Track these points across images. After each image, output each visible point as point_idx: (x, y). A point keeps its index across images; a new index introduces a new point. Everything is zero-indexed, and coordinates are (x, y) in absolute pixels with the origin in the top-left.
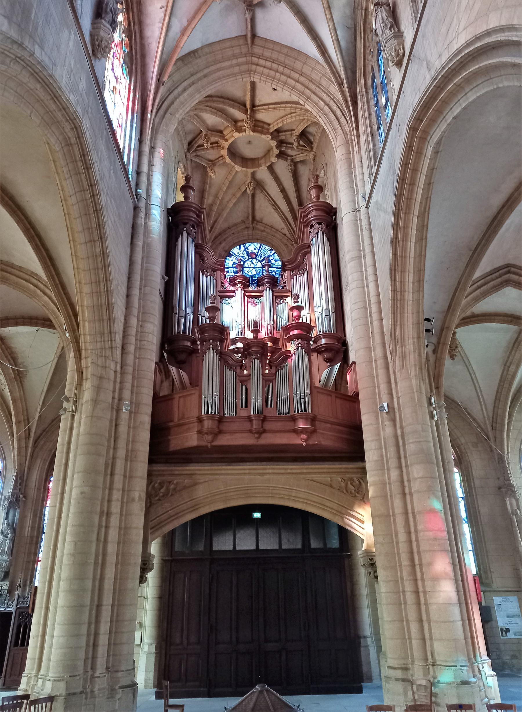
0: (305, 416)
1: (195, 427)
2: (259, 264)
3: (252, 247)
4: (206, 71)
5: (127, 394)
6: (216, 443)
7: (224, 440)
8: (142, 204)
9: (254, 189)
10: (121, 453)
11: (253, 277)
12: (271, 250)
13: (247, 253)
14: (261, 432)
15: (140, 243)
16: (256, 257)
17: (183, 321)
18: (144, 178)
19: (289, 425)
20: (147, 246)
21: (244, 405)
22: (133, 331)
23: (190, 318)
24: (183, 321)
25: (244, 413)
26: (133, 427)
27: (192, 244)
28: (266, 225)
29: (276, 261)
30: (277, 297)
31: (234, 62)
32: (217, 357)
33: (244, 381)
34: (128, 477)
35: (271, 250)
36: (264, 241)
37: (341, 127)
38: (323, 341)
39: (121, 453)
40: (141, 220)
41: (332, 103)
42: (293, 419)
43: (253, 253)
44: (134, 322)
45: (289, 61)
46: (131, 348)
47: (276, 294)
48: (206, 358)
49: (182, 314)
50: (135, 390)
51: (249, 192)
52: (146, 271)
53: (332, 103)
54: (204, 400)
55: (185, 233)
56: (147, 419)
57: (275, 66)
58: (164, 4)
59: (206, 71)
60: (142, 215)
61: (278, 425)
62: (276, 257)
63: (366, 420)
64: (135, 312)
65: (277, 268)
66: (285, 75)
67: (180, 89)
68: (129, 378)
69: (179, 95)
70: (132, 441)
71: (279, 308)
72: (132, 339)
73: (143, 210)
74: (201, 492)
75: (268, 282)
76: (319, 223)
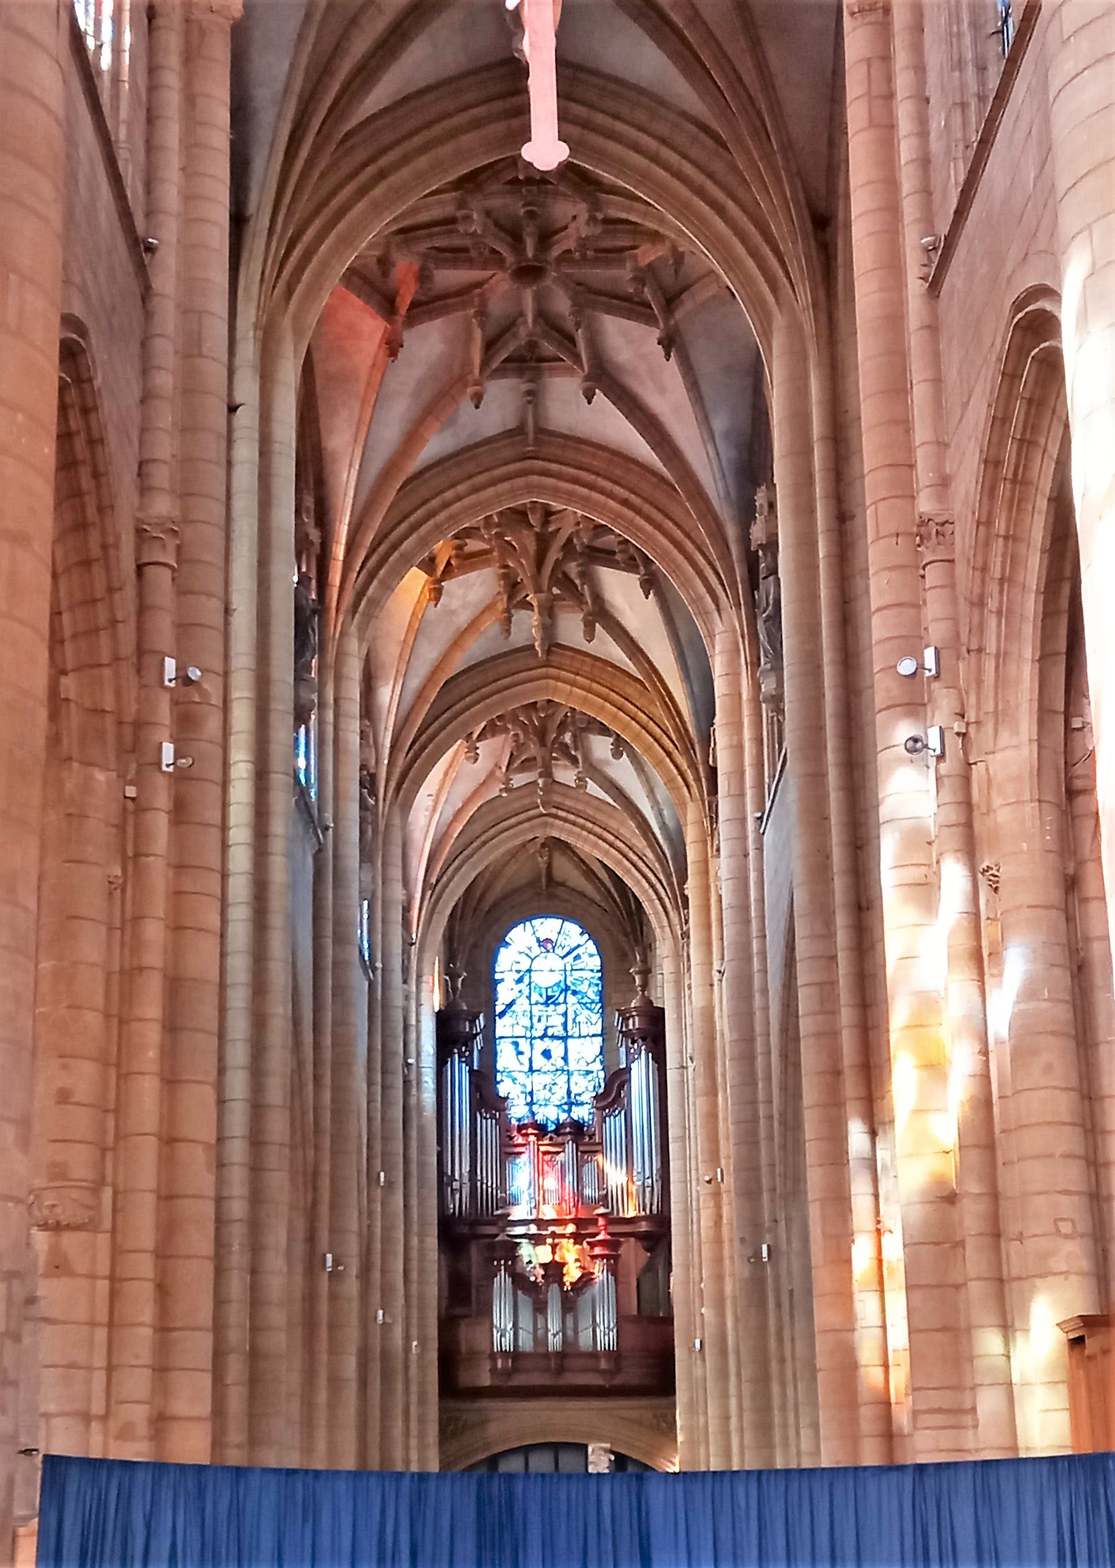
0: (608, 1353)
1: (487, 1366)
2: (559, 964)
3: (548, 927)
4: (483, 838)
5: (414, 1331)
6: (510, 1383)
7: (519, 1380)
8: (413, 1077)
9: (550, 857)
10: (414, 1398)
11: (550, 990)
12: (582, 934)
13: (538, 940)
14: (561, 1370)
15: (414, 1133)
16: (554, 948)
17: (457, 1196)
18: (413, 1036)
19: (591, 1363)
20: (421, 1129)
21: (540, 1340)
22: (414, 1254)
23: (466, 1191)
24: (457, 1196)
25: (541, 1350)
26: (422, 1367)
27: (465, 1068)
28: (573, 890)
29: (591, 955)
30: (583, 1152)
31: (523, 816)
32: (509, 1280)
33: (540, 1308)
34: (422, 1421)
35: (582, 934)
36: (566, 916)
37: (670, 926)
38: (644, 1227)
39: (414, 1398)
40: (413, 1101)
41: (658, 886)
42: (594, 1355)
43: (548, 940)
44: (415, 1241)
45: (599, 816)
46: (414, 1275)
47: (581, 1148)
48: (496, 1280)
49: (456, 1185)
50: (422, 1326)
51: (542, 861)
52: (422, 1165)
53: (658, 886)
54: (496, 1335)
55: (456, 1056)
56: (433, 1355)
57: (581, 821)
58: (433, 792)
59: (483, 838)
60: (414, 1091)
61: (580, 1363)
62: (591, 947)
63: (679, 1353)
64: (415, 1228)
65: (592, 971)
66: (595, 835)
67: (449, 872)
68: (414, 1312)
69: (449, 881)
70: (422, 1383)
71: (586, 1168)
72: (414, 1264)
73: (414, 1083)
74: (493, 1429)
75: (569, 1133)
76: (644, 1039)
